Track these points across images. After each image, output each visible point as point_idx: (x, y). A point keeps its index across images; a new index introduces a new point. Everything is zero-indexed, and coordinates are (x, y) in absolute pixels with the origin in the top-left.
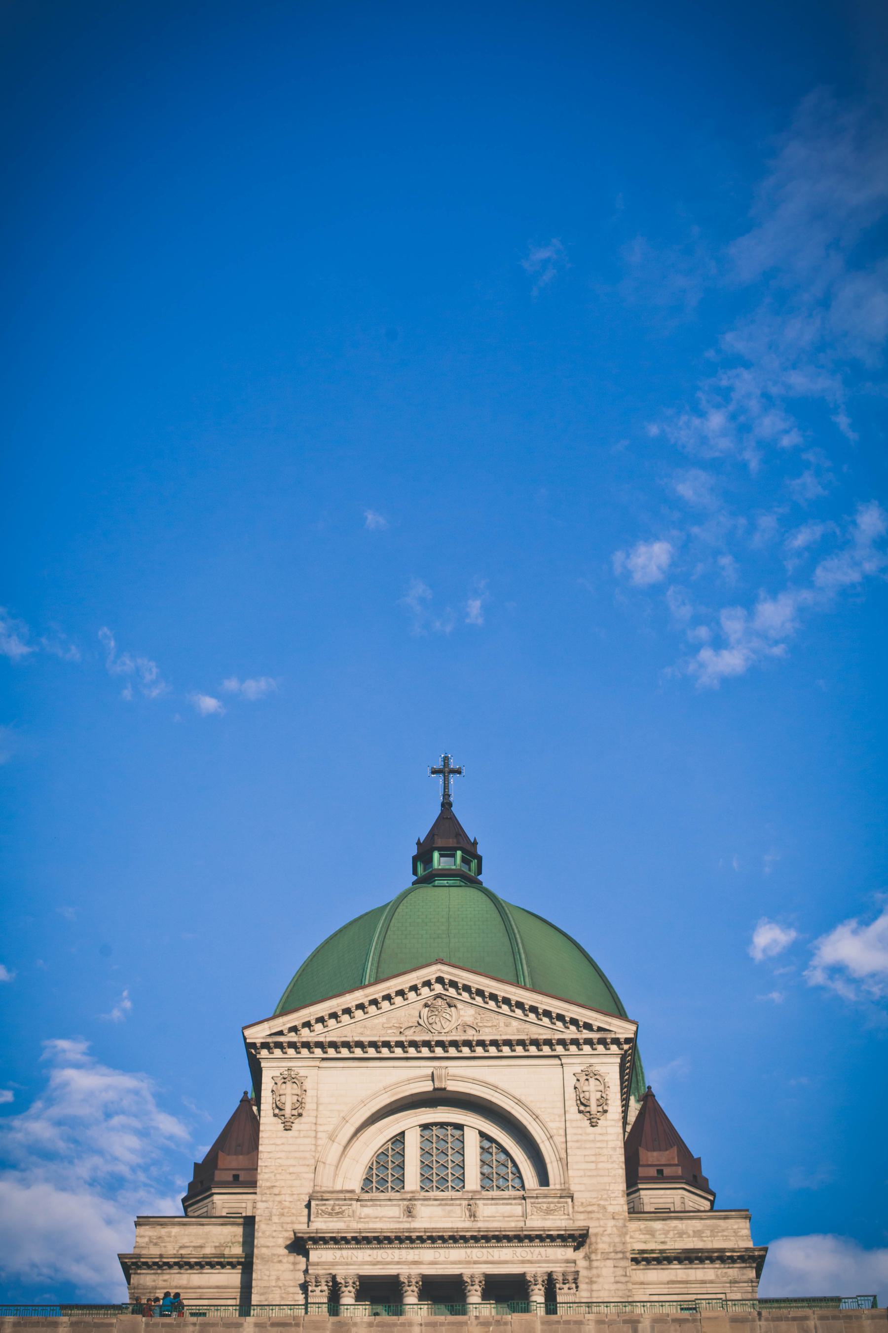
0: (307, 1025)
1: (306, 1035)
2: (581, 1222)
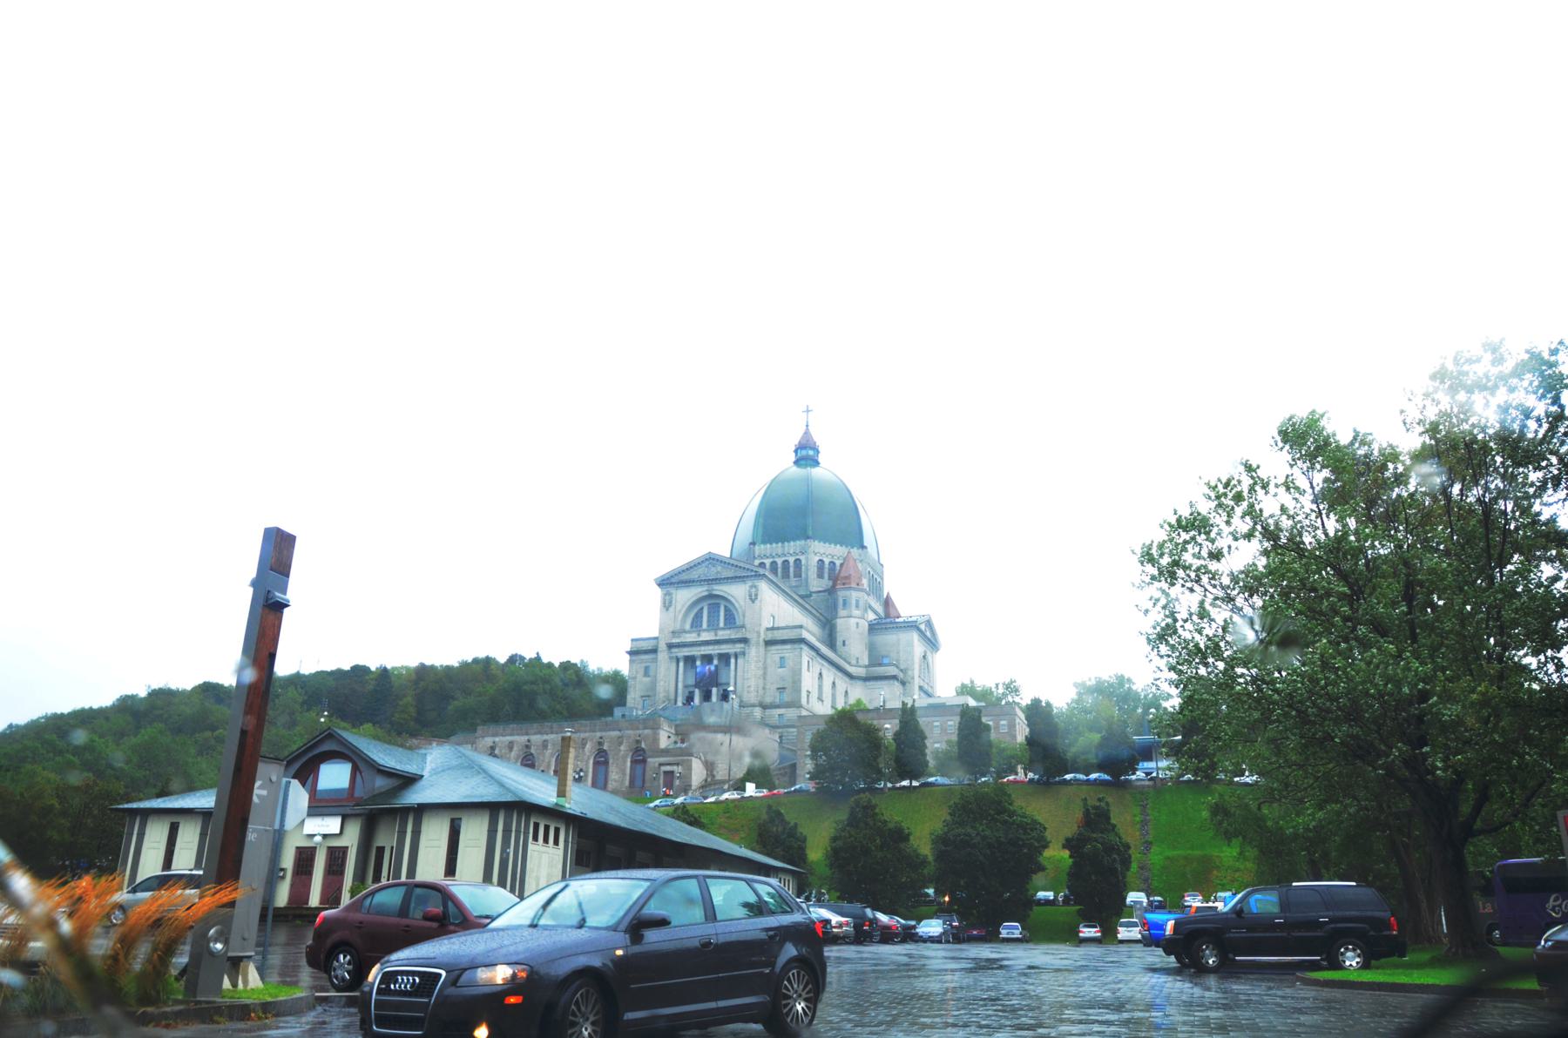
1: (673, 580)
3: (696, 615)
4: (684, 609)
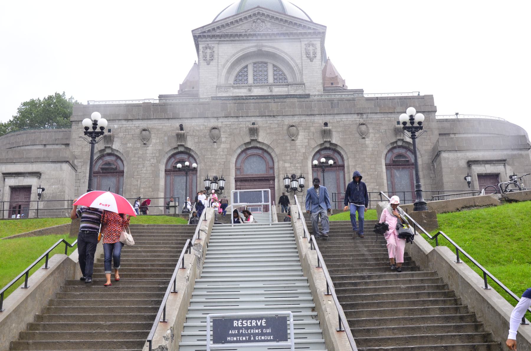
0: (214, 29)
1: (213, 33)
2: (307, 92)
3: (238, 75)
4: (229, 64)
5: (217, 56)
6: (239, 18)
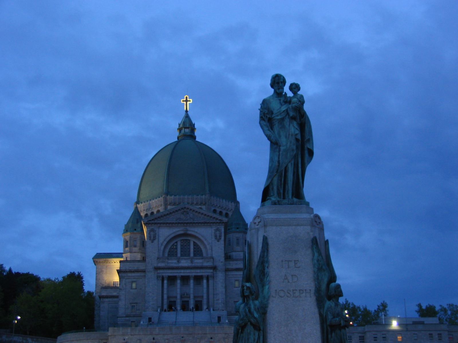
1: (156, 221)
4: (165, 242)
5: (158, 237)
6: (172, 211)
